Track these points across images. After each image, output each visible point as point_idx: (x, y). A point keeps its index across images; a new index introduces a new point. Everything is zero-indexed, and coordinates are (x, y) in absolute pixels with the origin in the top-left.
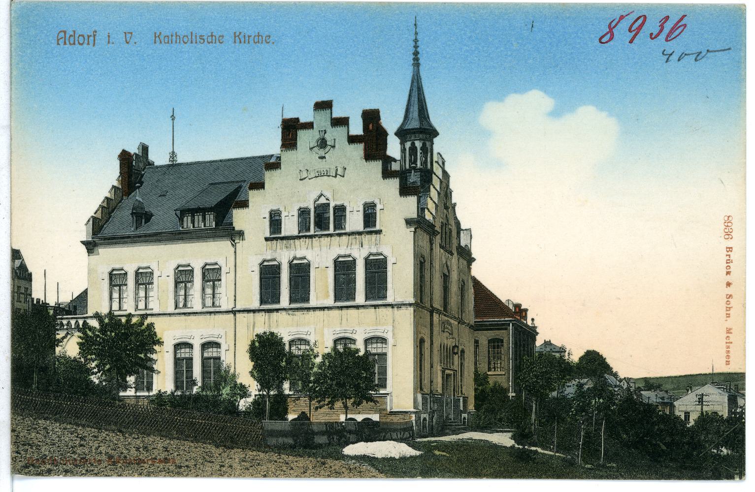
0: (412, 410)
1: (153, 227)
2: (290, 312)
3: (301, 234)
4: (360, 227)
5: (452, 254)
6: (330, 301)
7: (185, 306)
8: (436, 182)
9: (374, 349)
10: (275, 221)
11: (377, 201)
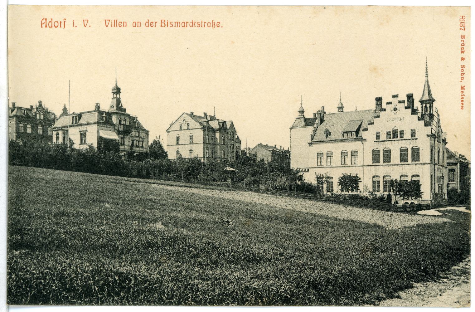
0: (430, 199)
1: (332, 137)
2: (384, 166)
3: (387, 140)
4: (410, 137)
5: (440, 143)
6: (399, 162)
7: (344, 164)
8: (435, 118)
9: (414, 179)
10: (378, 137)
11: (416, 129)
